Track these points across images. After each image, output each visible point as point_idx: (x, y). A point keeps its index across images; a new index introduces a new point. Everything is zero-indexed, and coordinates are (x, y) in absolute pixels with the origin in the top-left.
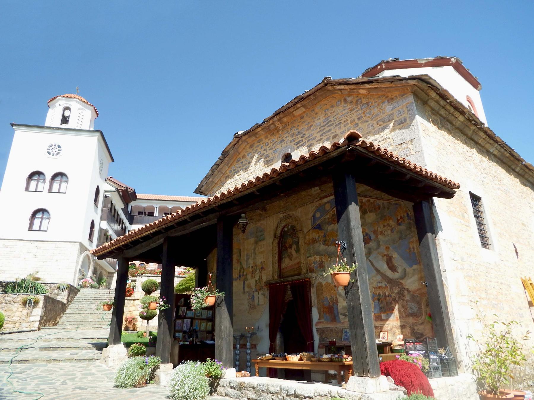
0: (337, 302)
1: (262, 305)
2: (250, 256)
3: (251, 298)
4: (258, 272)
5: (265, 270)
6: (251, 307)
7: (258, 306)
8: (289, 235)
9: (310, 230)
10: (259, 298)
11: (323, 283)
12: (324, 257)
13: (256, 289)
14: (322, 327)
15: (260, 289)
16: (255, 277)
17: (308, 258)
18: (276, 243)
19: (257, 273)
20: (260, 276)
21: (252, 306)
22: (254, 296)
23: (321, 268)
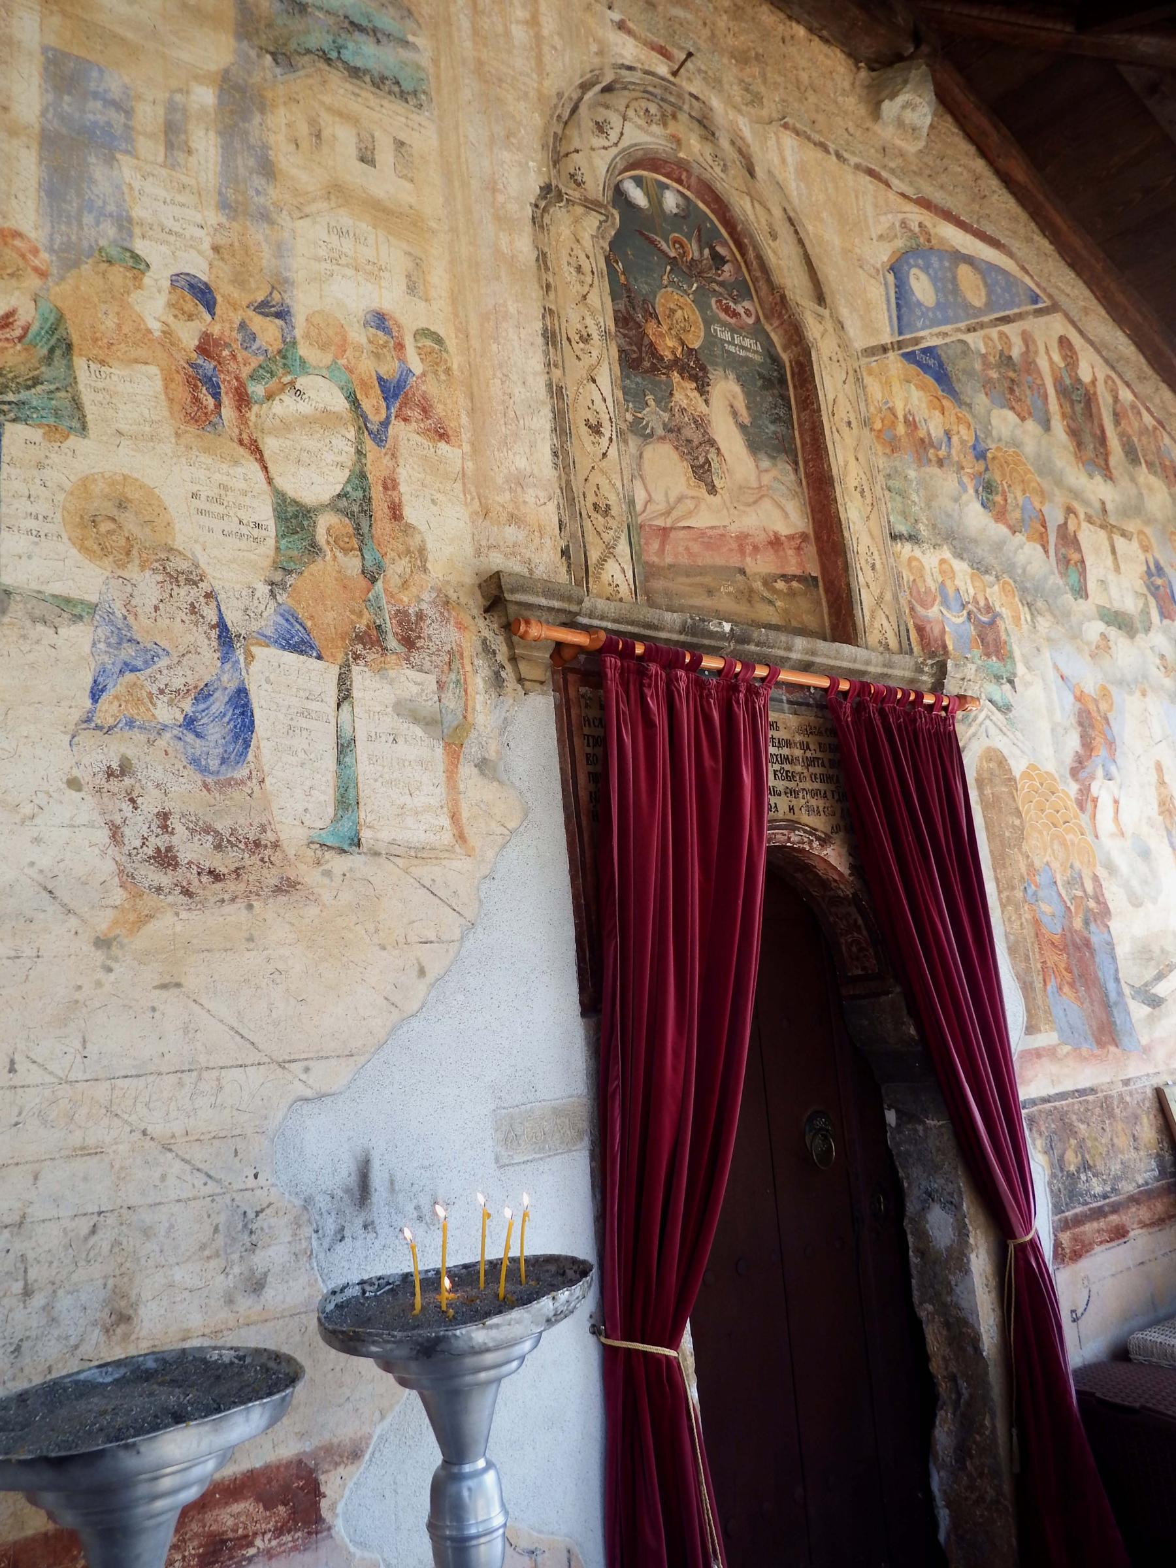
0: (1104, 913)
1: (420, 854)
2: (148, 116)
3: (166, 713)
4: (324, 420)
5: (442, 435)
6: (166, 859)
7: (338, 864)
8: (673, 261)
9: (885, 349)
10: (344, 747)
11: (1012, 762)
12: (996, 587)
13: (290, 617)
14: (1052, 1091)
15: (372, 638)
16: (256, 450)
17: (895, 537)
18: (587, 242)
19: (286, 406)
20: (361, 476)
21: (191, 850)
22: (241, 701)
23: (988, 655)
